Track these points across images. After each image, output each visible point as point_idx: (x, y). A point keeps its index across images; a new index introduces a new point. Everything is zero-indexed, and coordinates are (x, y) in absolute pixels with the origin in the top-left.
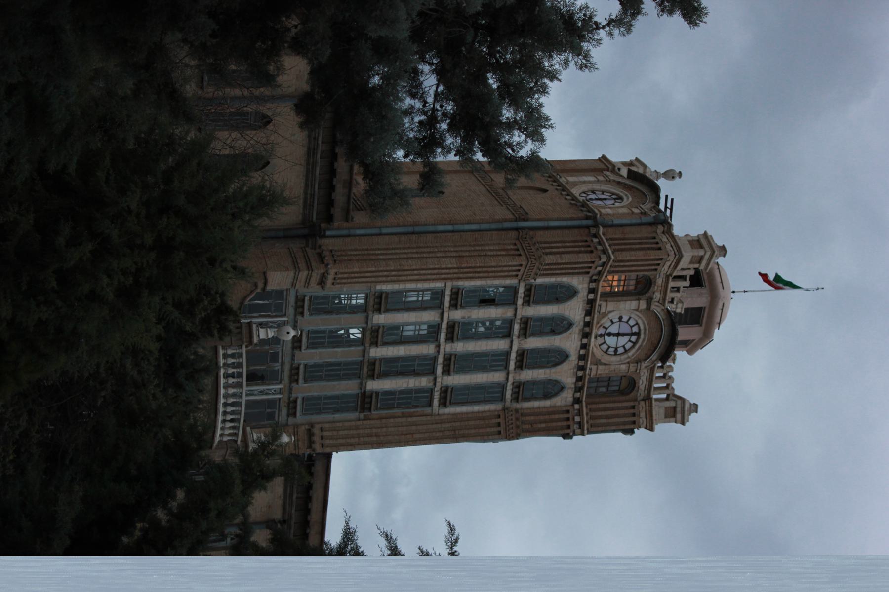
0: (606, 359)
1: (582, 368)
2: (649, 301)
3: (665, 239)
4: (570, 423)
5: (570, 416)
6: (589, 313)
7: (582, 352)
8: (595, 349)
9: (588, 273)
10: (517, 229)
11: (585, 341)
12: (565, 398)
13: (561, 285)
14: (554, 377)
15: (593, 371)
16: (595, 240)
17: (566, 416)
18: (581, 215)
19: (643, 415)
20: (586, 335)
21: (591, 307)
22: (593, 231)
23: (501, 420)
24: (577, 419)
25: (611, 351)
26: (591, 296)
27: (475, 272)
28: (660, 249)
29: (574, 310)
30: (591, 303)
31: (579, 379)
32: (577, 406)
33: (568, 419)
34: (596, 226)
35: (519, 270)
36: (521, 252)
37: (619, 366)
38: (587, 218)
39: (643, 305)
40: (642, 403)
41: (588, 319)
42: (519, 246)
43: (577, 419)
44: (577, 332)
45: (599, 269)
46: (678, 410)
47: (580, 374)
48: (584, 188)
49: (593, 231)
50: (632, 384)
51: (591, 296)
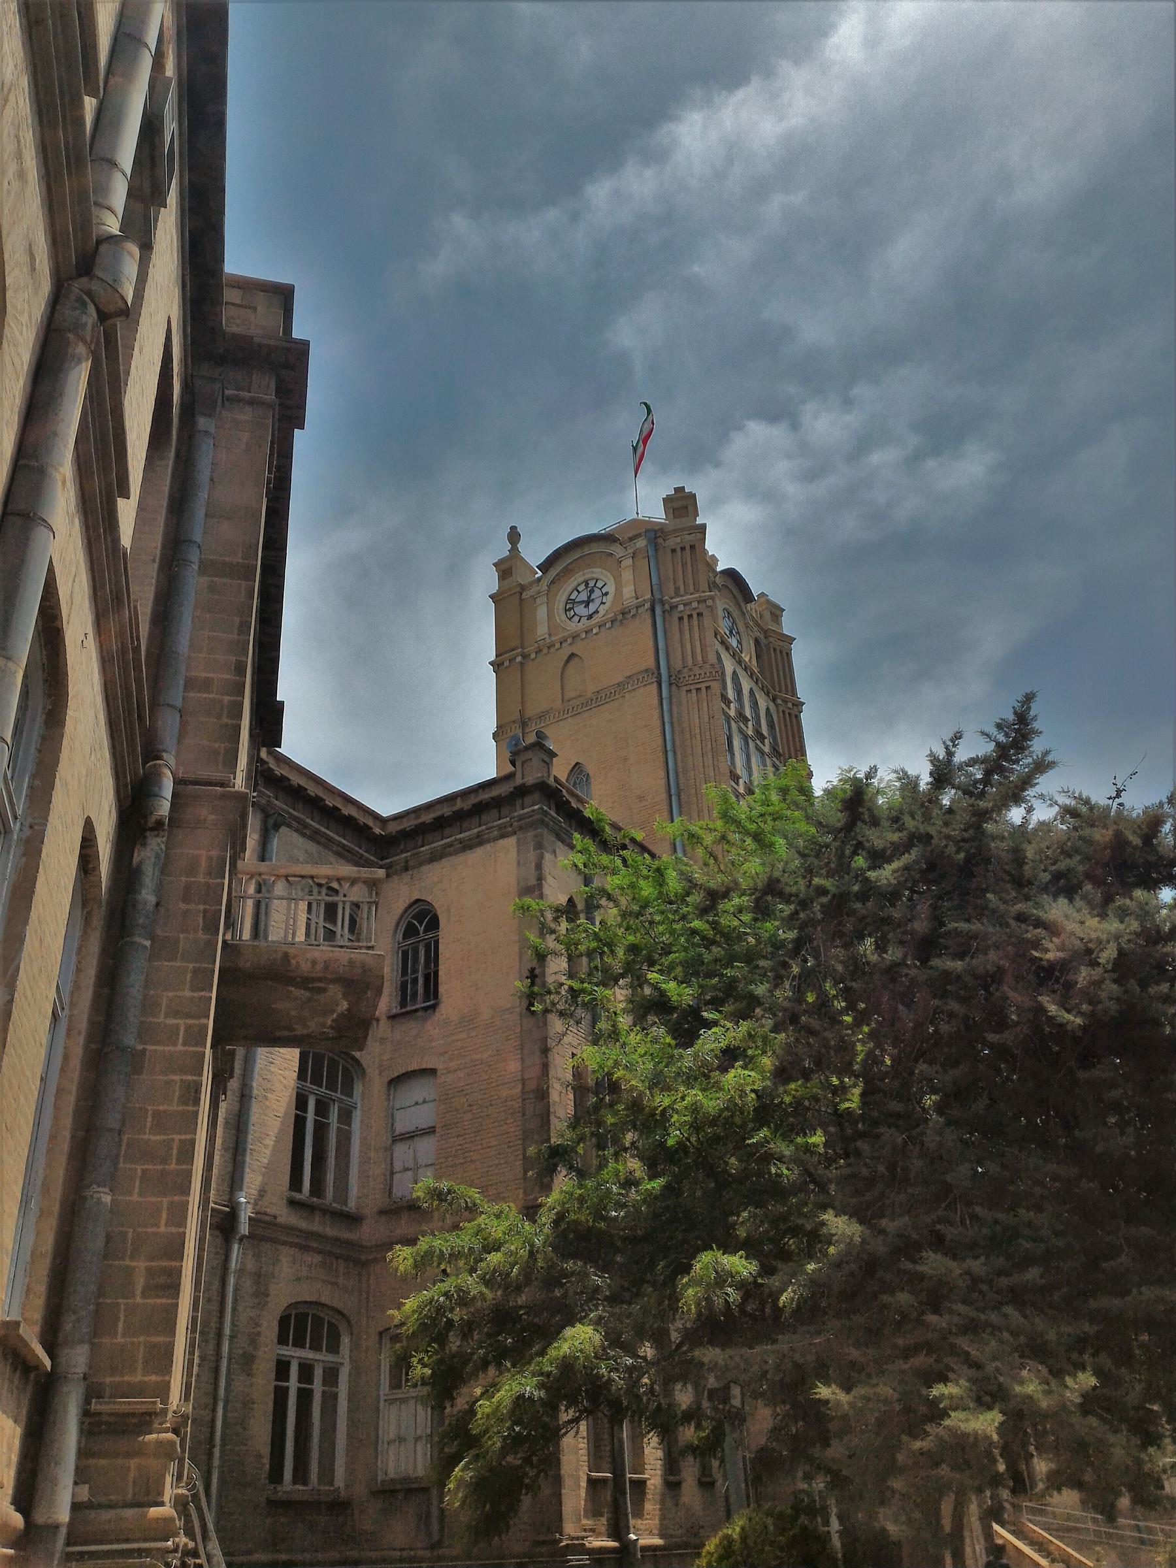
3: (678, 540)
4: (793, 713)
5: (787, 711)
10: (670, 684)
16: (681, 608)
18: (647, 617)
28: (692, 547)
32: (779, 701)
34: (662, 603)
36: (703, 686)
38: (653, 610)
40: (771, 639)
42: (692, 687)
43: (790, 705)
48: (560, 617)
49: (667, 607)
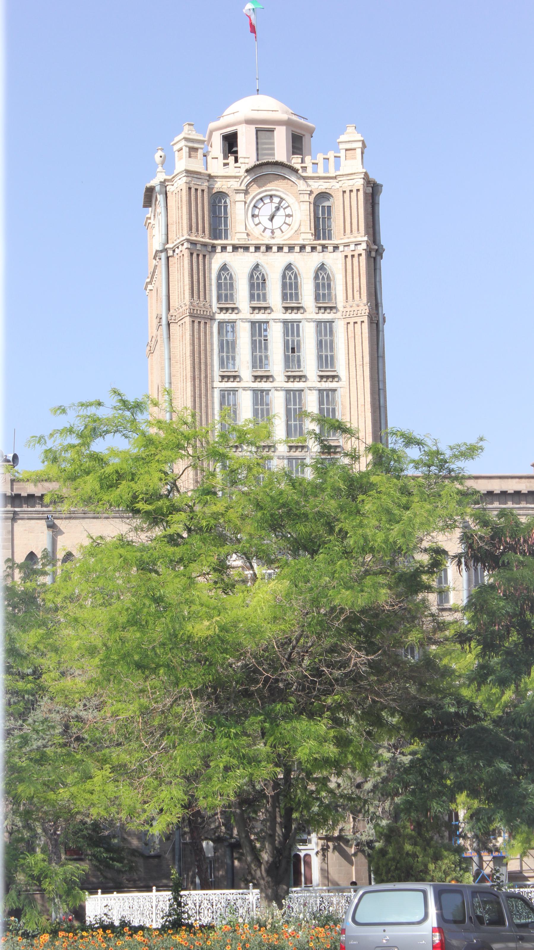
0: (295, 227)
1: (303, 248)
2: (237, 191)
4: (356, 254)
6: (246, 248)
7: (286, 249)
8: (286, 237)
9: (204, 256)
10: (169, 324)
11: (275, 249)
12: (334, 262)
13: (219, 277)
14: (312, 275)
15: (307, 238)
17: (350, 258)
19: (351, 182)
20: (269, 248)
21: (241, 247)
22: (170, 253)
23: (352, 321)
24: (352, 247)
25: (288, 220)
26: (229, 249)
27: (200, 363)
29: (241, 265)
30: (235, 248)
31: (313, 248)
32: (341, 248)
33: (353, 256)
34: (165, 250)
35: (199, 322)
37: (301, 213)
39: (241, 197)
41: (252, 249)
43: (352, 247)
44: (265, 257)
45: (199, 247)
46: (348, 146)
47: (308, 249)
50: (324, 196)
51: (229, 249)
